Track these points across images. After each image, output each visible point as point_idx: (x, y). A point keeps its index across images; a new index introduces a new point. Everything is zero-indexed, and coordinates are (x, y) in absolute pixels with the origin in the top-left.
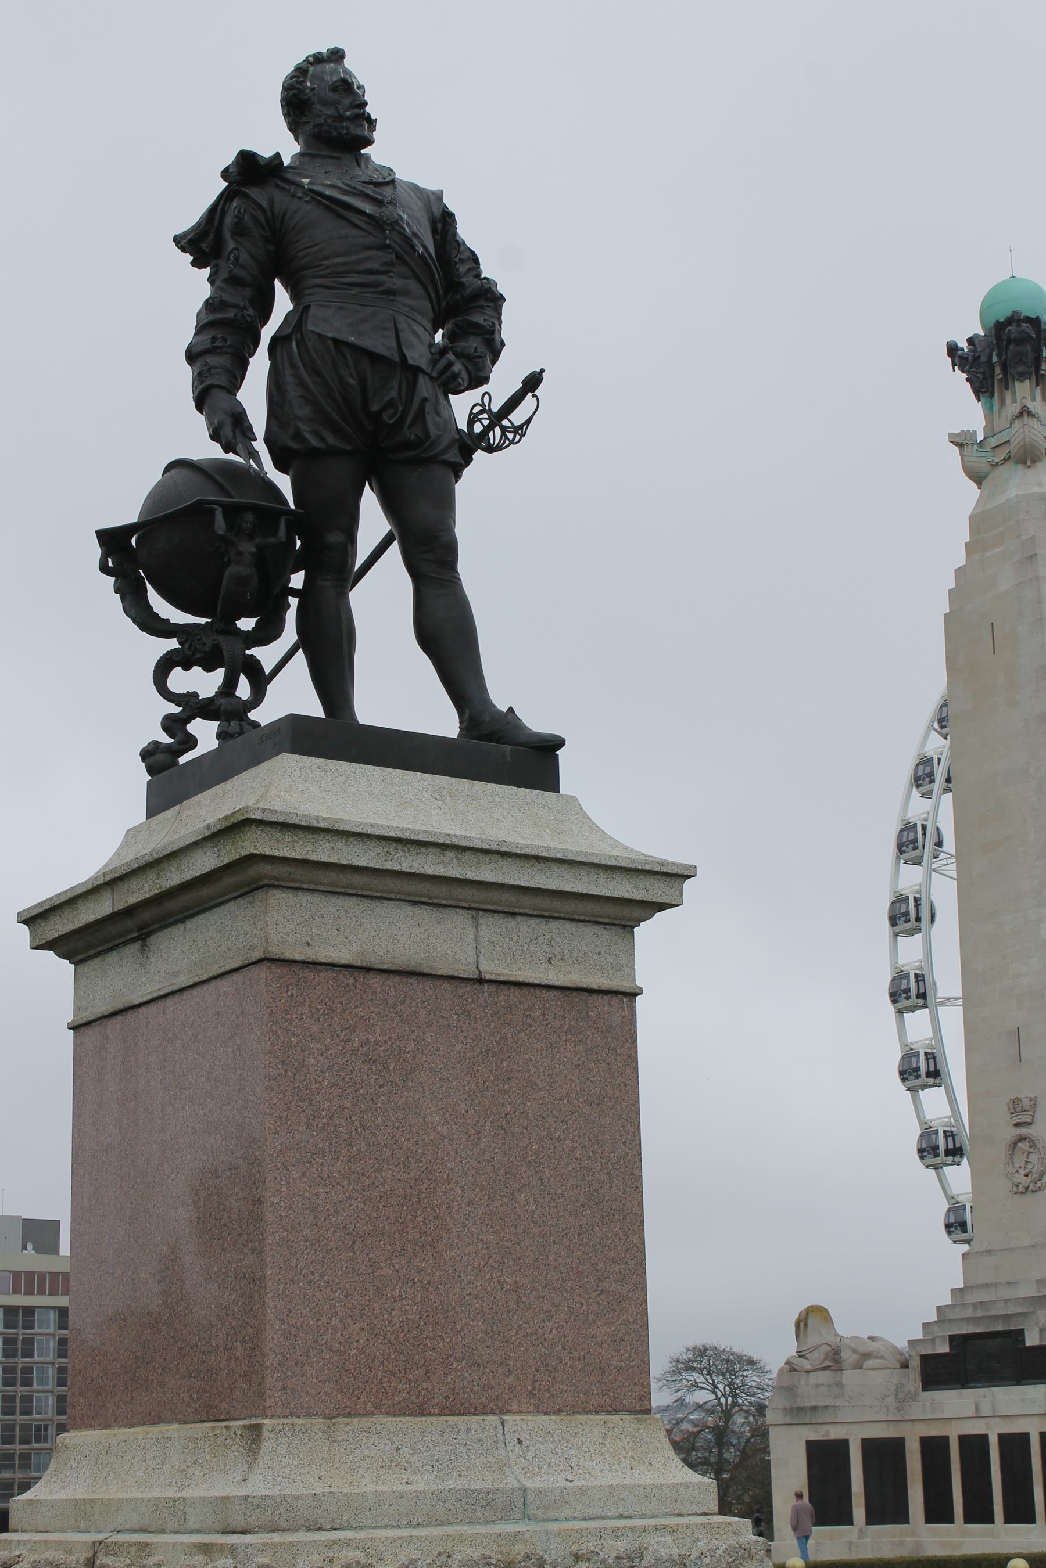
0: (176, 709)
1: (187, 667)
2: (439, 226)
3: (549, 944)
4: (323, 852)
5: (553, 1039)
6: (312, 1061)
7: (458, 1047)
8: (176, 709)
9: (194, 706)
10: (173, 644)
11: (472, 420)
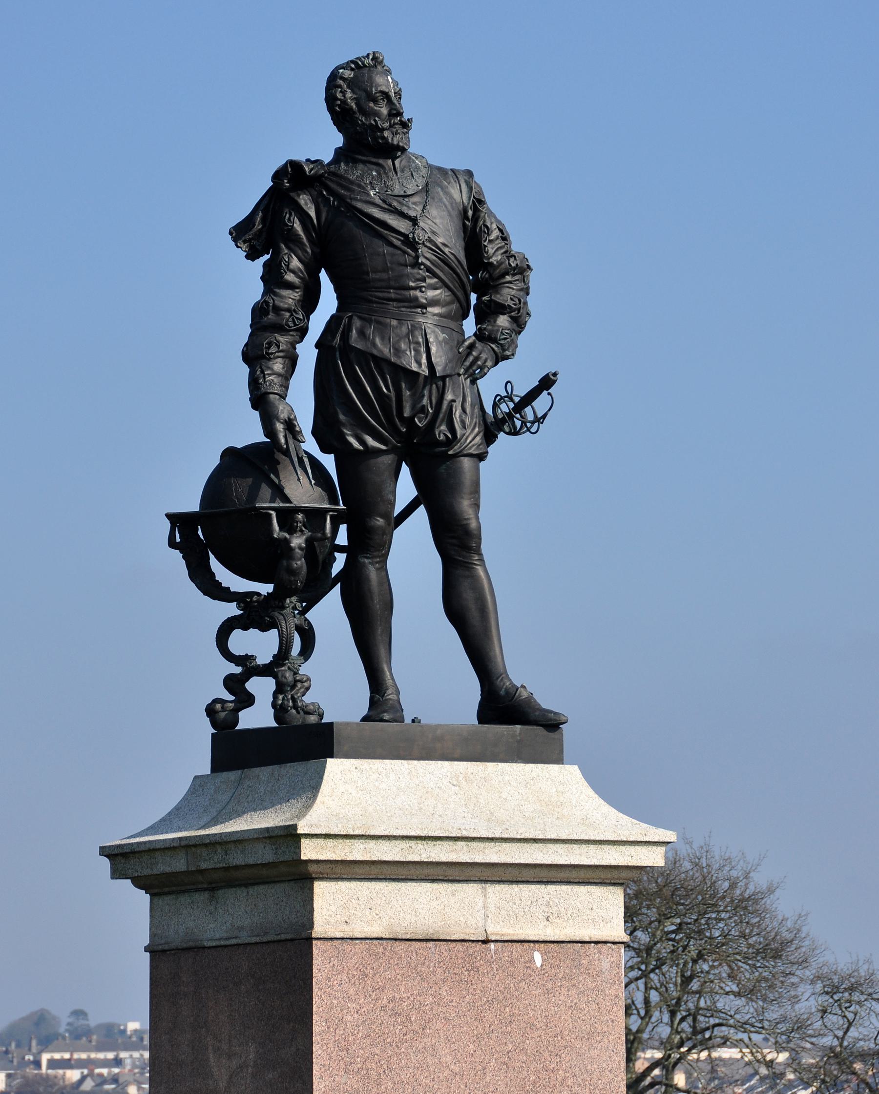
0: (238, 670)
1: (245, 628)
2: (470, 213)
3: (548, 904)
4: (358, 852)
5: (549, 986)
6: (349, 1018)
7: (468, 998)
8: (238, 670)
9: (249, 667)
10: (232, 610)
11: (495, 406)
